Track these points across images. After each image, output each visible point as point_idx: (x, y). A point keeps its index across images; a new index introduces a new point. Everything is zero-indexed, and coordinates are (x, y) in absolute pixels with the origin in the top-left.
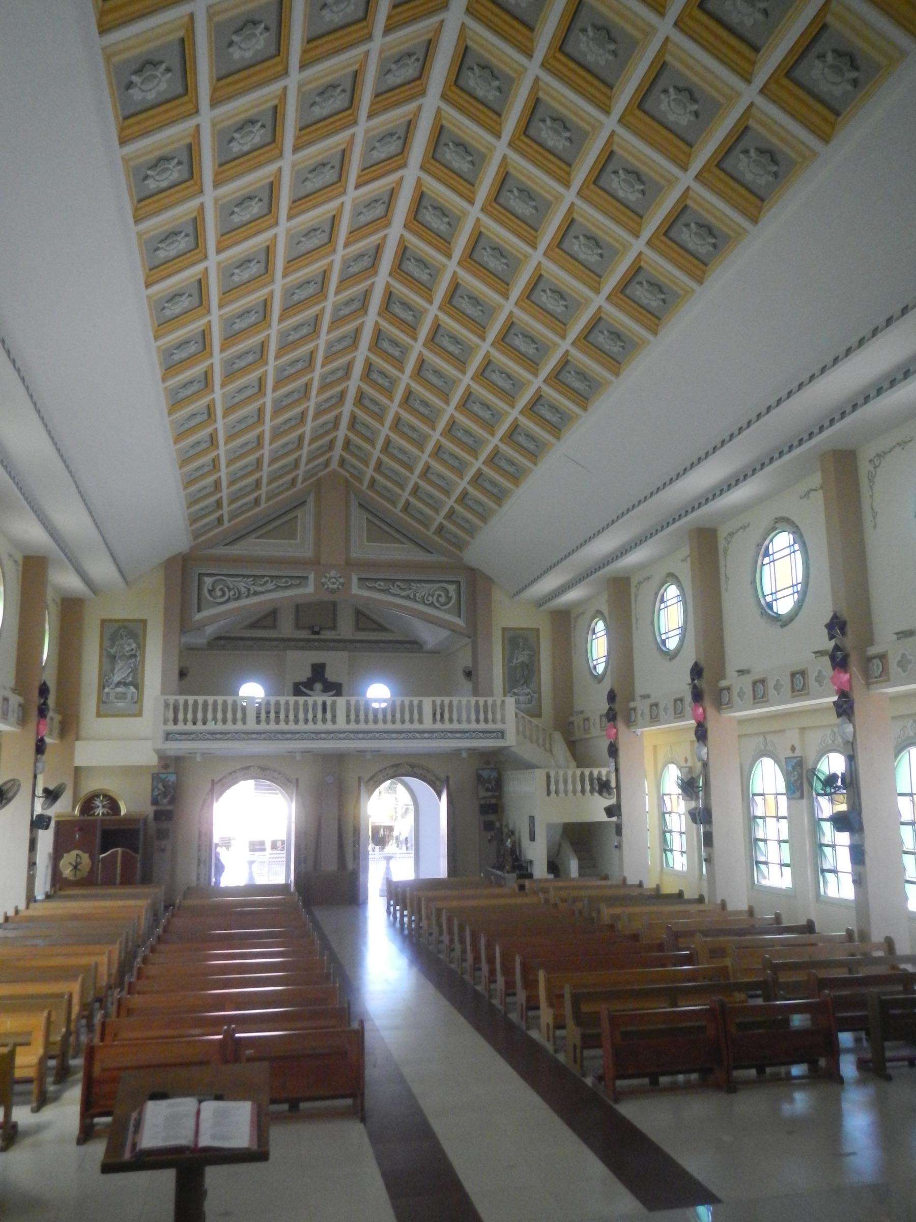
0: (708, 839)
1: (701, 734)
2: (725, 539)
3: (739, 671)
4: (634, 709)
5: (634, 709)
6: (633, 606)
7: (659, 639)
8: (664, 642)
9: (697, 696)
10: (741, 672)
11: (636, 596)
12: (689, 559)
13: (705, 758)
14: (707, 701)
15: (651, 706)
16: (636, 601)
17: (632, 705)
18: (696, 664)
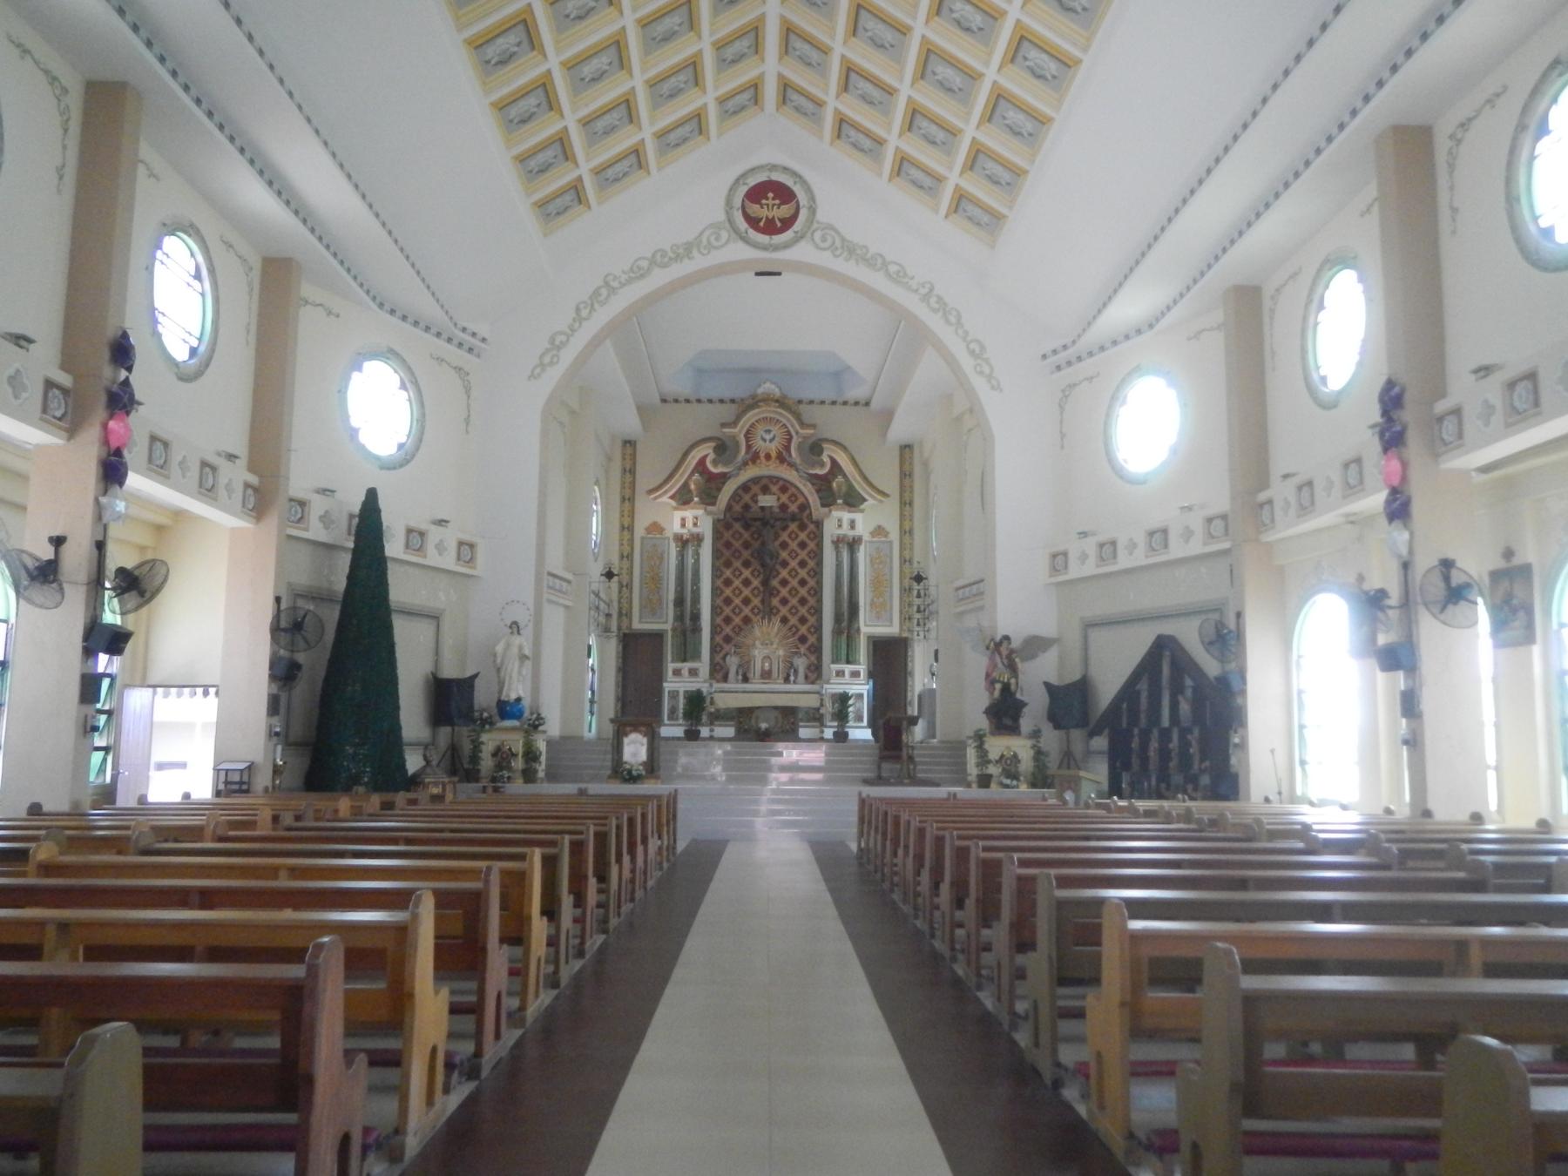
0: (1410, 705)
1: (1399, 509)
2: (1451, 137)
3: (1476, 371)
4: (1270, 502)
5: (1270, 502)
6: (1266, 328)
7: (1315, 377)
8: (1324, 379)
9: (1392, 438)
10: (1484, 371)
11: (1272, 311)
12: (1376, 209)
13: (1404, 551)
14: (1414, 445)
15: (1300, 488)
16: (1272, 318)
17: (1262, 497)
18: (1390, 384)
